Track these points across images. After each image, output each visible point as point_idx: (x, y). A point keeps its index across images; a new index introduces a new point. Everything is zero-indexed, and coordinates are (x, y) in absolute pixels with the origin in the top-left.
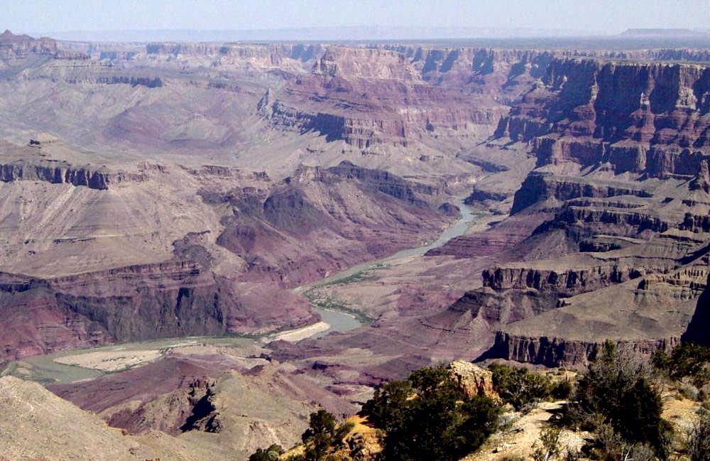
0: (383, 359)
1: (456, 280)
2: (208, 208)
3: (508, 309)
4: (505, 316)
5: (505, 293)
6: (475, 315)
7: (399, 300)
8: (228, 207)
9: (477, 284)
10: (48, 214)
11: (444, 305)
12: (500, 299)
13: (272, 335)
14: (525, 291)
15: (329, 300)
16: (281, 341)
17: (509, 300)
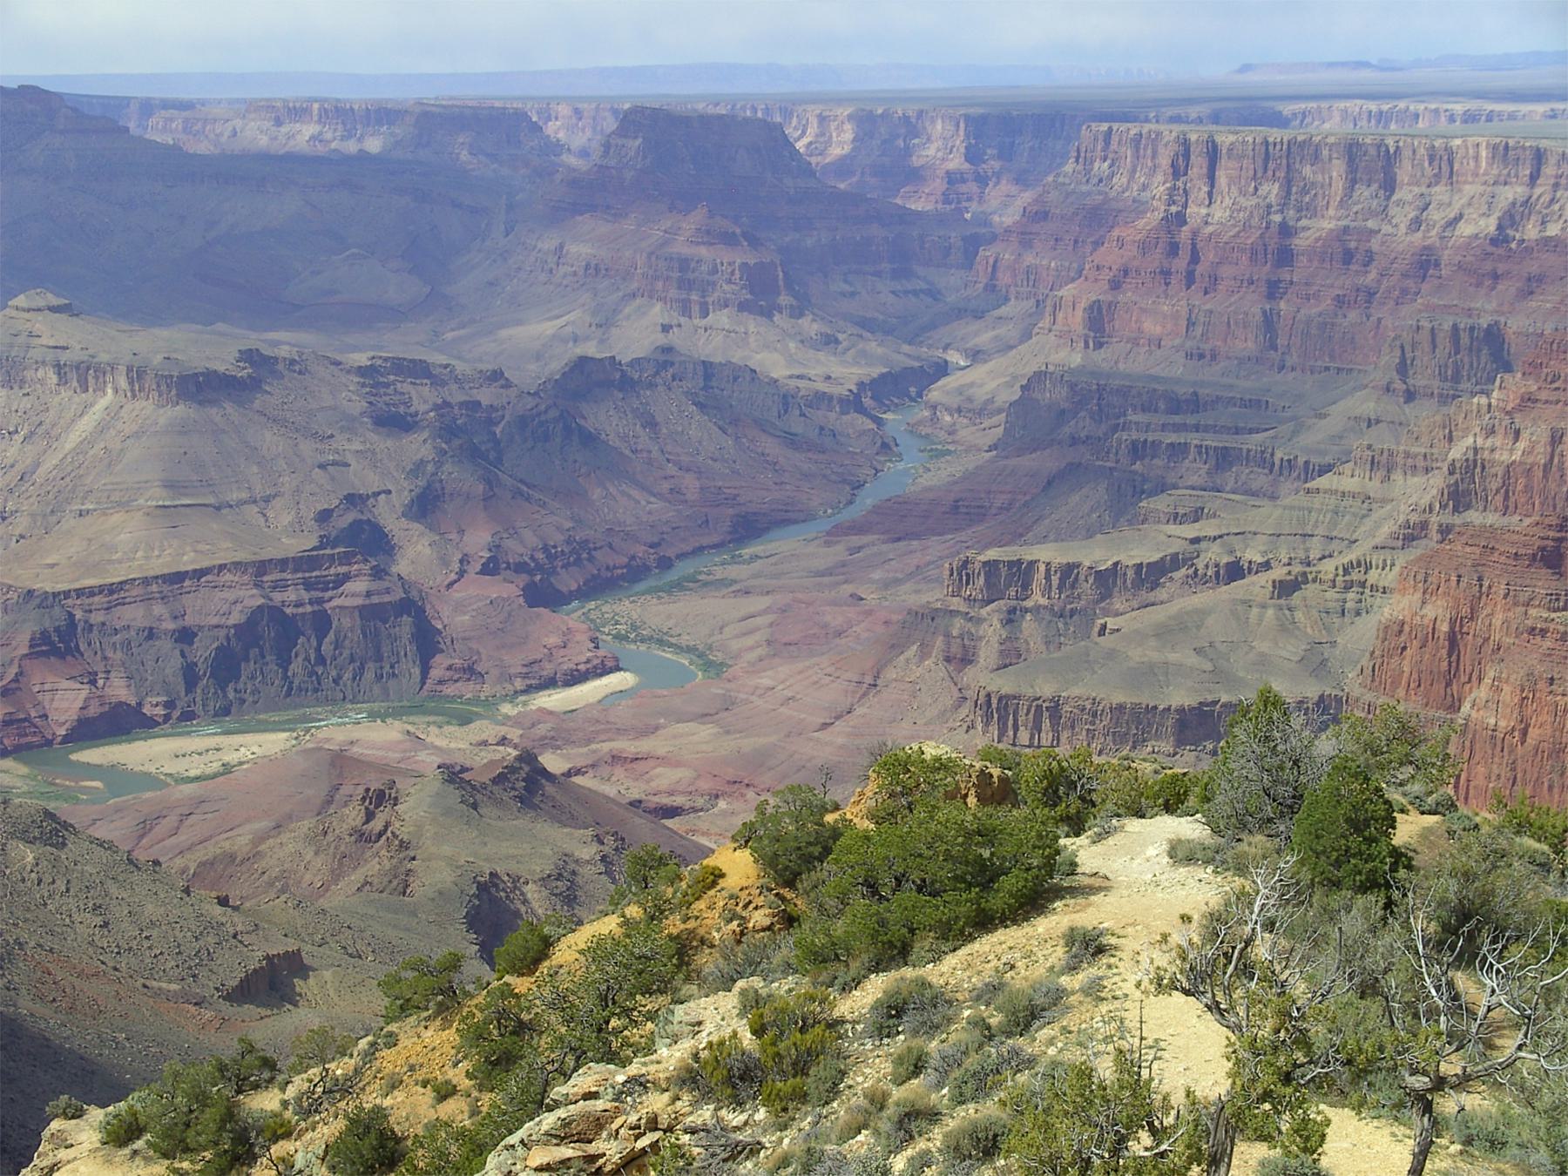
0: (748, 744)
1: (886, 585)
2: (383, 443)
3: (994, 641)
4: (987, 654)
5: (988, 608)
6: (923, 655)
7: (771, 625)
8: (425, 441)
9: (934, 596)
10: (51, 461)
11: (865, 635)
12: (979, 621)
13: (522, 698)
14: (1029, 604)
15: (634, 627)
16: (541, 710)
17: (996, 623)
